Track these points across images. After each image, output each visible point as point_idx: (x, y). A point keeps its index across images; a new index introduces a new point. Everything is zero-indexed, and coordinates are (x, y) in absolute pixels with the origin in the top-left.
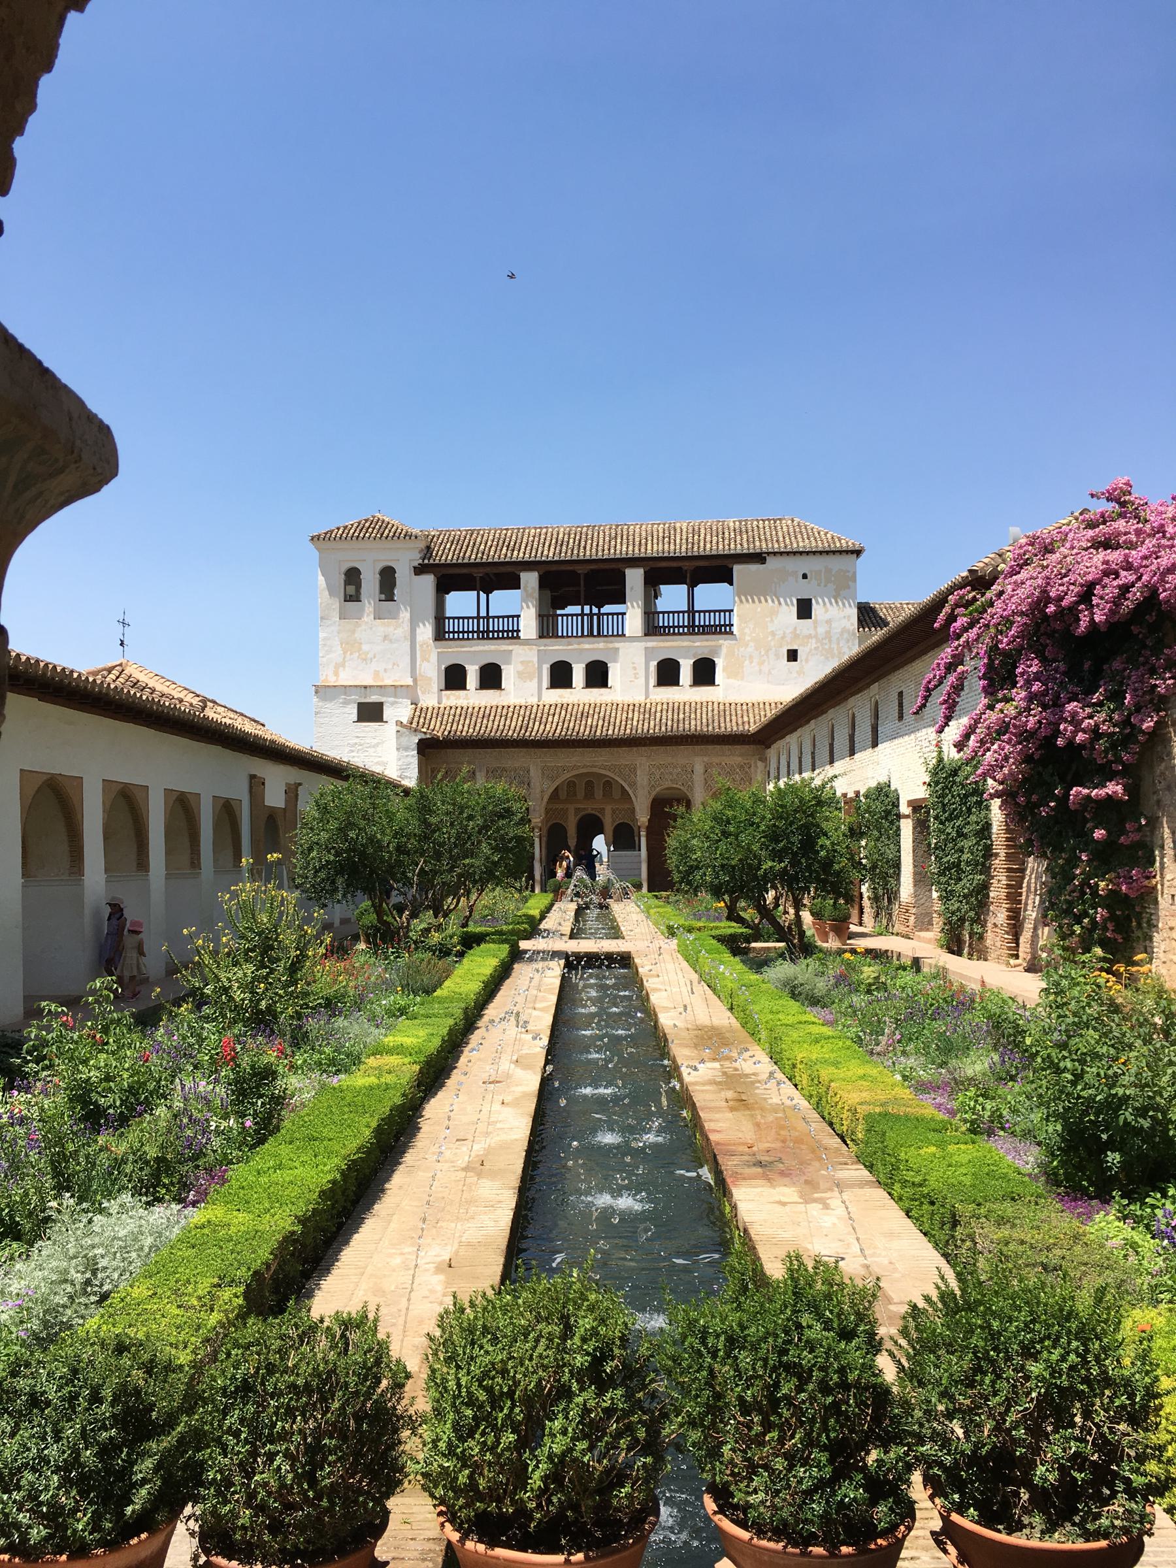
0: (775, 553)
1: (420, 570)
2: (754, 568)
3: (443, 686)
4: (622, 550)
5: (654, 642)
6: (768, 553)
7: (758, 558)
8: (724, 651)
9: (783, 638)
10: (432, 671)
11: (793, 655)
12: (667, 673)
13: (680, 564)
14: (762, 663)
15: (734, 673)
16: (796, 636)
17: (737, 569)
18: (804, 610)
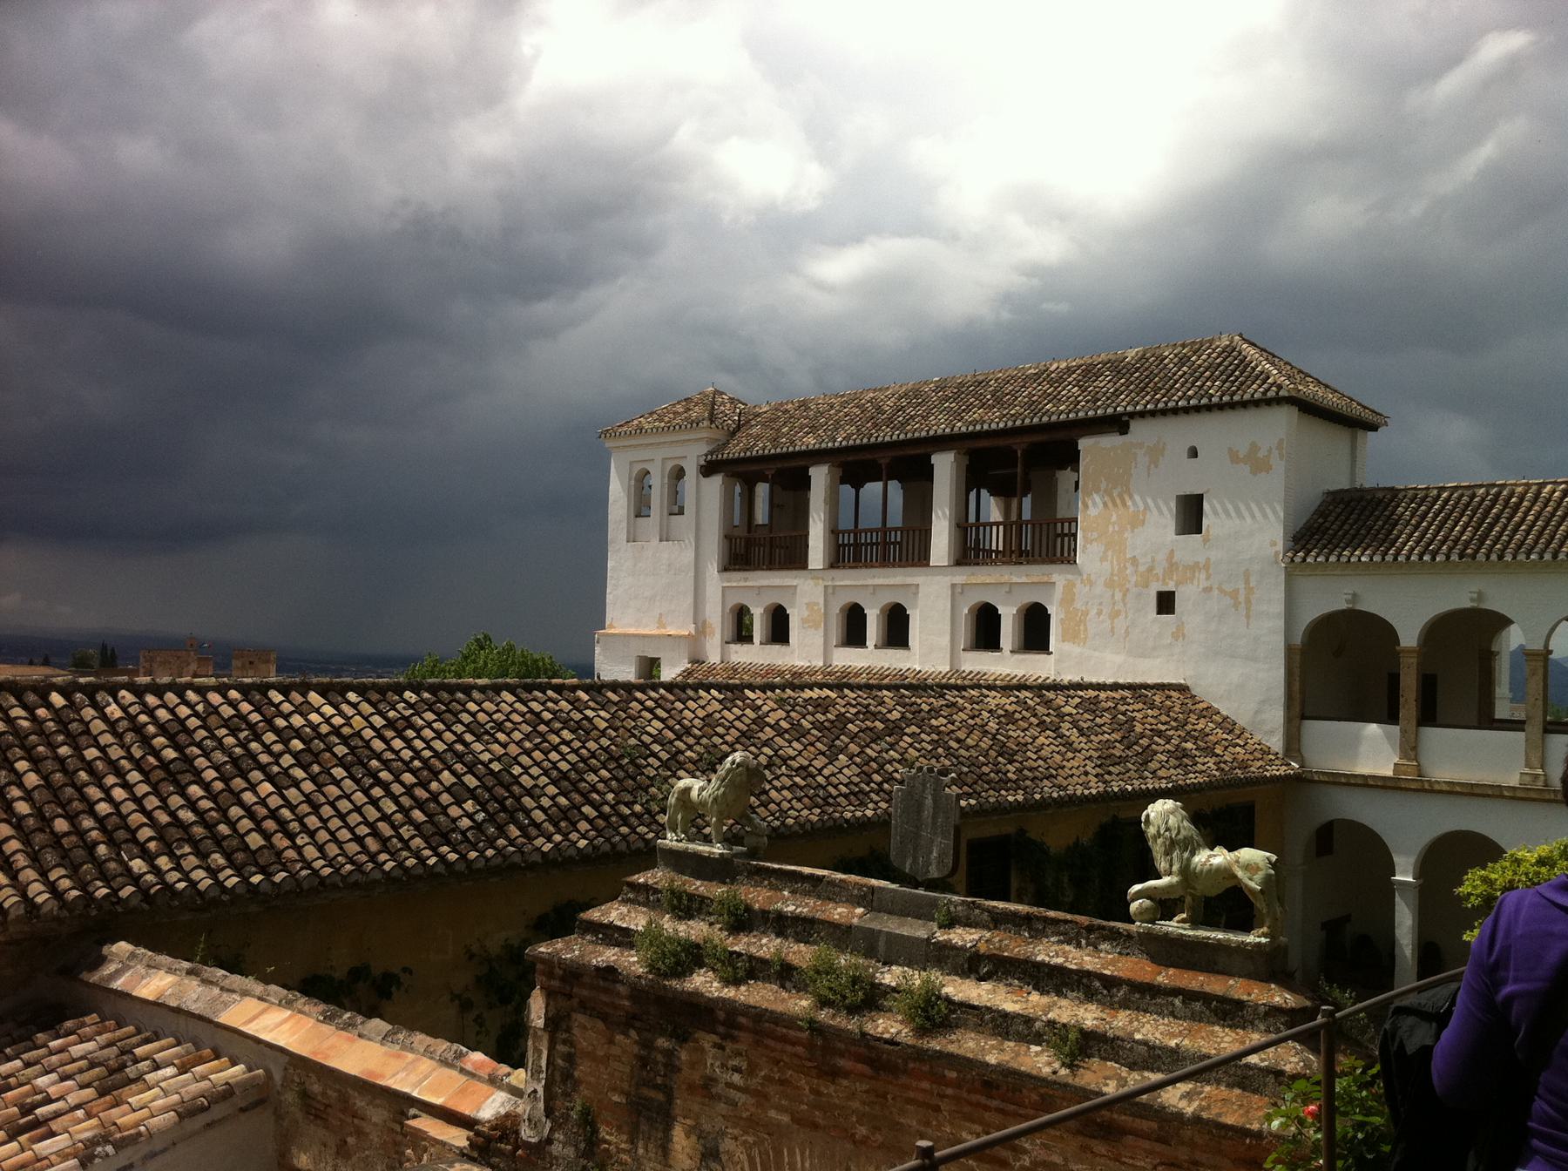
0: (1142, 414)
1: (708, 469)
2: (1109, 442)
3: (729, 634)
4: (940, 425)
5: (963, 576)
6: (1132, 415)
7: (1117, 424)
8: (1059, 592)
9: (1151, 569)
10: (716, 616)
11: (1166, 603)
12: (985, 630)
13: (1001, 442)
14: (1114, 615)
15: (1070, 636)
16: (1172, 566)
17: (1084, 444)
18: (1191, 515)
